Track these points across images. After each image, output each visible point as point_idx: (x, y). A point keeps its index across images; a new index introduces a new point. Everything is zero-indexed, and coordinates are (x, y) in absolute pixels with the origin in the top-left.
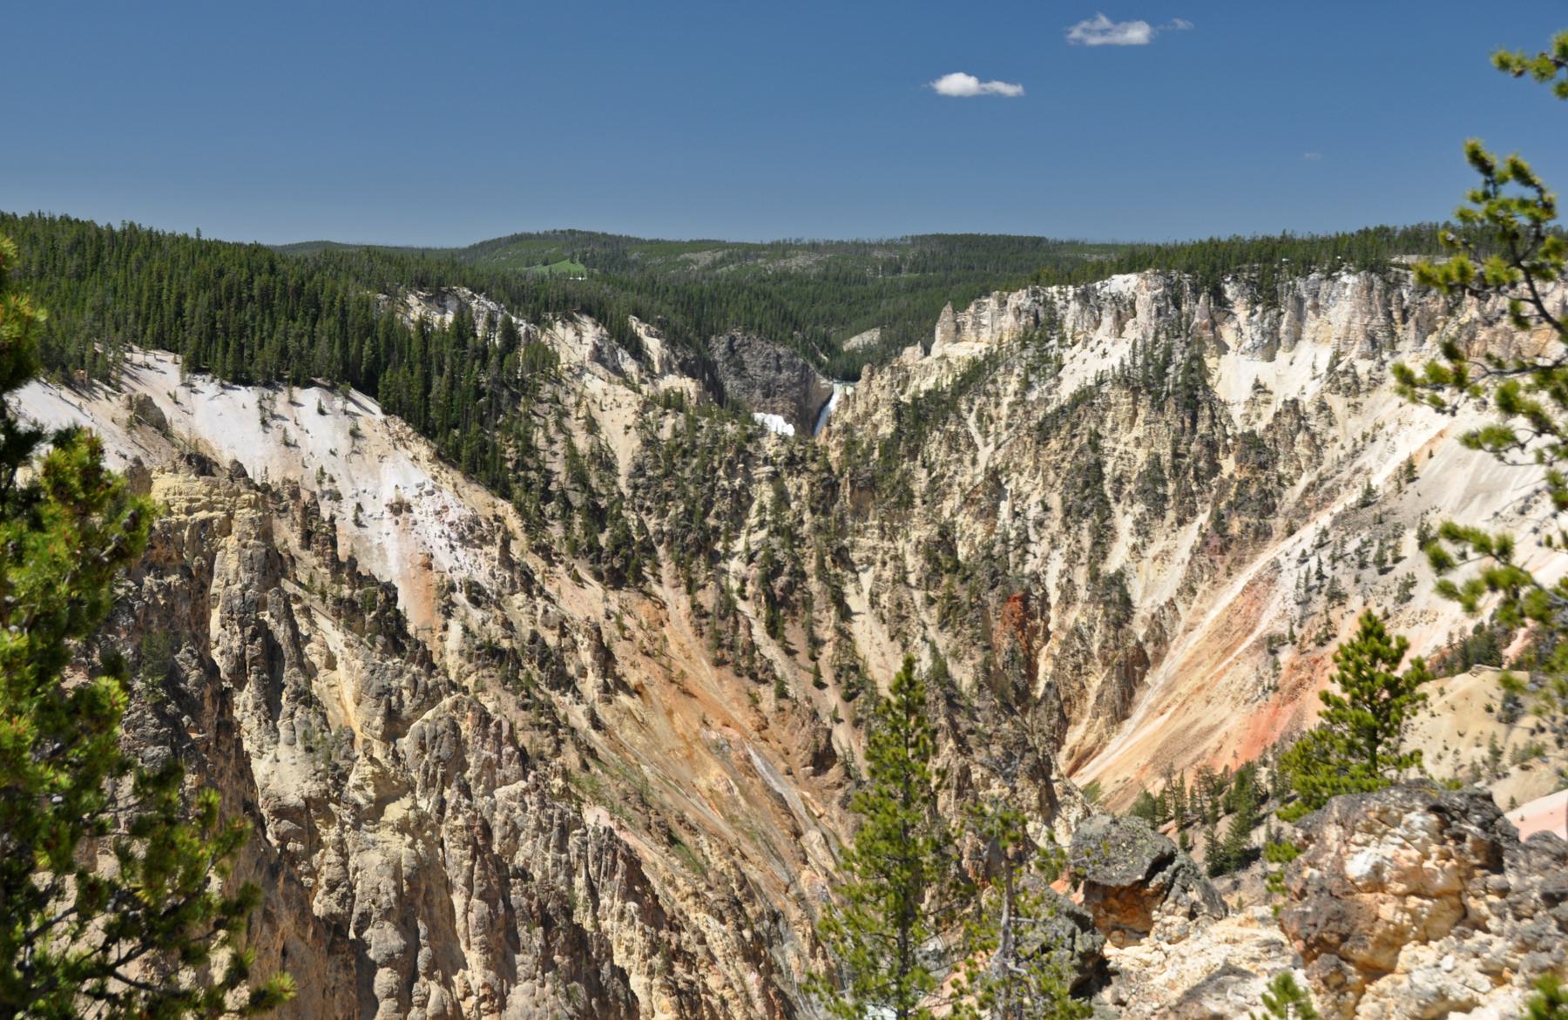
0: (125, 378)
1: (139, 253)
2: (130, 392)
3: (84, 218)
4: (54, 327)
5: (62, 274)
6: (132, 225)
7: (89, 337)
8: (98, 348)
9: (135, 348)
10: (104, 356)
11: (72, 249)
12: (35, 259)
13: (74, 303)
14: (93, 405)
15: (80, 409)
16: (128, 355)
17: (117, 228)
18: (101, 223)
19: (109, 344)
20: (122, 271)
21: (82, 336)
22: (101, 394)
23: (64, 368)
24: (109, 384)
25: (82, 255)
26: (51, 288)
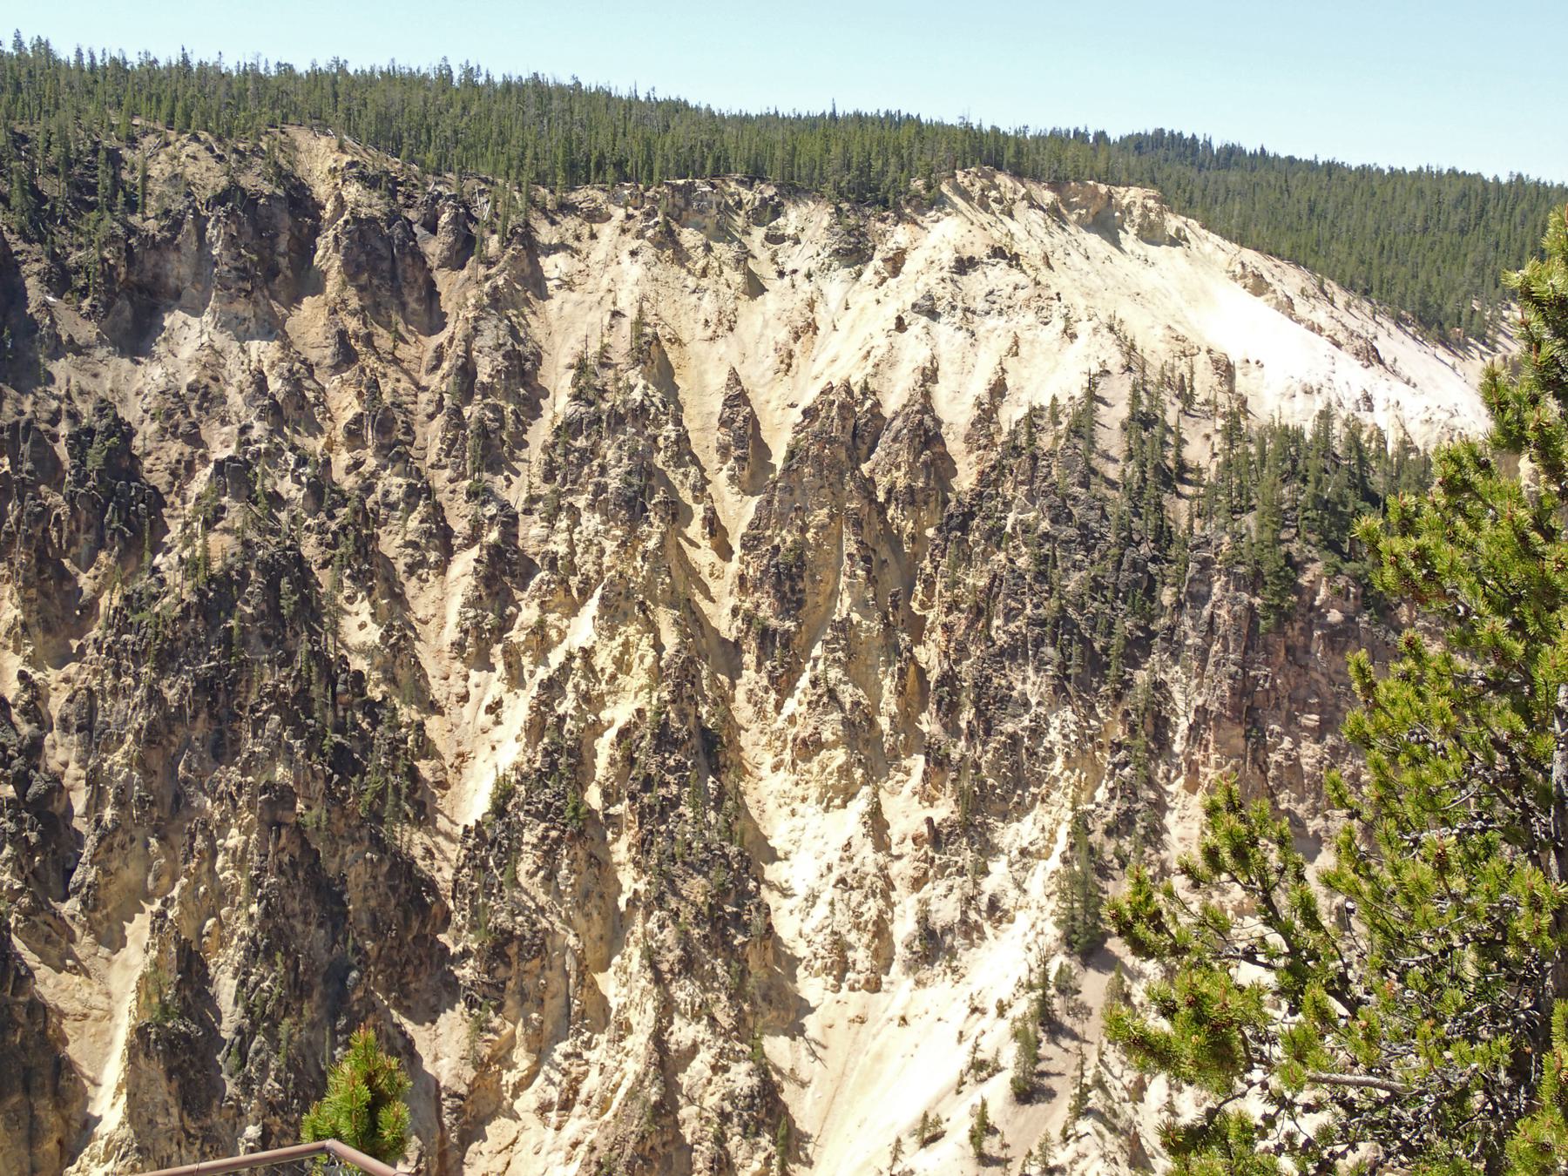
0: (1501, 338)
1: (1524, 205)
2: (1505, 352)
3: (1471, 170)
4: (1434, 283)
5: (1446, 229)
6: (1519, 176)
7: (1466, 295)
8: (1476, 305)
9: (1513, 305)
10: (1481, 314)
11: (1458, 202)
12: (1420, 214)
13: (1455, 259)
14: (1466, 364)
15: (1454, 368)
16: (1506, 313)
17: (1504, 179)
18: (1488, 176)
19: (1487, 302)
20: (1505, 225)
21: (1460, 293)
22: (1476, 354)
23: (1441, 325)
24: (1484, 343)
25: (1467, 209)
26: (1434, 243)
